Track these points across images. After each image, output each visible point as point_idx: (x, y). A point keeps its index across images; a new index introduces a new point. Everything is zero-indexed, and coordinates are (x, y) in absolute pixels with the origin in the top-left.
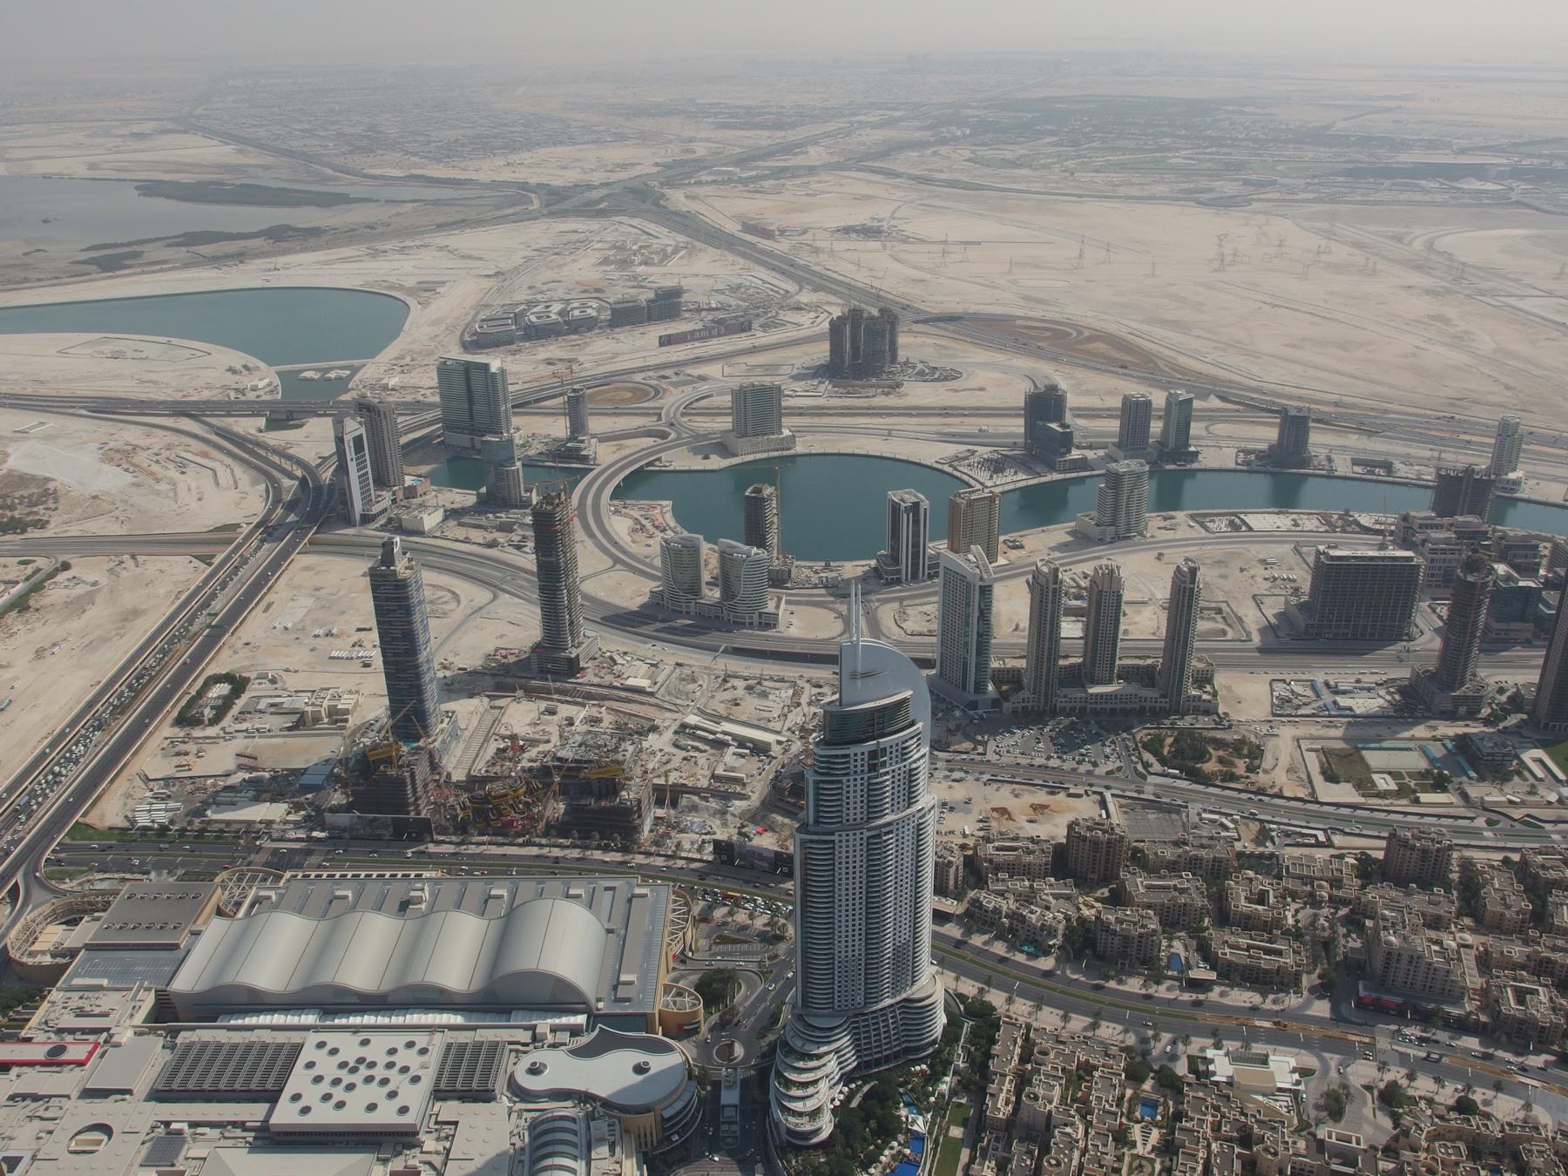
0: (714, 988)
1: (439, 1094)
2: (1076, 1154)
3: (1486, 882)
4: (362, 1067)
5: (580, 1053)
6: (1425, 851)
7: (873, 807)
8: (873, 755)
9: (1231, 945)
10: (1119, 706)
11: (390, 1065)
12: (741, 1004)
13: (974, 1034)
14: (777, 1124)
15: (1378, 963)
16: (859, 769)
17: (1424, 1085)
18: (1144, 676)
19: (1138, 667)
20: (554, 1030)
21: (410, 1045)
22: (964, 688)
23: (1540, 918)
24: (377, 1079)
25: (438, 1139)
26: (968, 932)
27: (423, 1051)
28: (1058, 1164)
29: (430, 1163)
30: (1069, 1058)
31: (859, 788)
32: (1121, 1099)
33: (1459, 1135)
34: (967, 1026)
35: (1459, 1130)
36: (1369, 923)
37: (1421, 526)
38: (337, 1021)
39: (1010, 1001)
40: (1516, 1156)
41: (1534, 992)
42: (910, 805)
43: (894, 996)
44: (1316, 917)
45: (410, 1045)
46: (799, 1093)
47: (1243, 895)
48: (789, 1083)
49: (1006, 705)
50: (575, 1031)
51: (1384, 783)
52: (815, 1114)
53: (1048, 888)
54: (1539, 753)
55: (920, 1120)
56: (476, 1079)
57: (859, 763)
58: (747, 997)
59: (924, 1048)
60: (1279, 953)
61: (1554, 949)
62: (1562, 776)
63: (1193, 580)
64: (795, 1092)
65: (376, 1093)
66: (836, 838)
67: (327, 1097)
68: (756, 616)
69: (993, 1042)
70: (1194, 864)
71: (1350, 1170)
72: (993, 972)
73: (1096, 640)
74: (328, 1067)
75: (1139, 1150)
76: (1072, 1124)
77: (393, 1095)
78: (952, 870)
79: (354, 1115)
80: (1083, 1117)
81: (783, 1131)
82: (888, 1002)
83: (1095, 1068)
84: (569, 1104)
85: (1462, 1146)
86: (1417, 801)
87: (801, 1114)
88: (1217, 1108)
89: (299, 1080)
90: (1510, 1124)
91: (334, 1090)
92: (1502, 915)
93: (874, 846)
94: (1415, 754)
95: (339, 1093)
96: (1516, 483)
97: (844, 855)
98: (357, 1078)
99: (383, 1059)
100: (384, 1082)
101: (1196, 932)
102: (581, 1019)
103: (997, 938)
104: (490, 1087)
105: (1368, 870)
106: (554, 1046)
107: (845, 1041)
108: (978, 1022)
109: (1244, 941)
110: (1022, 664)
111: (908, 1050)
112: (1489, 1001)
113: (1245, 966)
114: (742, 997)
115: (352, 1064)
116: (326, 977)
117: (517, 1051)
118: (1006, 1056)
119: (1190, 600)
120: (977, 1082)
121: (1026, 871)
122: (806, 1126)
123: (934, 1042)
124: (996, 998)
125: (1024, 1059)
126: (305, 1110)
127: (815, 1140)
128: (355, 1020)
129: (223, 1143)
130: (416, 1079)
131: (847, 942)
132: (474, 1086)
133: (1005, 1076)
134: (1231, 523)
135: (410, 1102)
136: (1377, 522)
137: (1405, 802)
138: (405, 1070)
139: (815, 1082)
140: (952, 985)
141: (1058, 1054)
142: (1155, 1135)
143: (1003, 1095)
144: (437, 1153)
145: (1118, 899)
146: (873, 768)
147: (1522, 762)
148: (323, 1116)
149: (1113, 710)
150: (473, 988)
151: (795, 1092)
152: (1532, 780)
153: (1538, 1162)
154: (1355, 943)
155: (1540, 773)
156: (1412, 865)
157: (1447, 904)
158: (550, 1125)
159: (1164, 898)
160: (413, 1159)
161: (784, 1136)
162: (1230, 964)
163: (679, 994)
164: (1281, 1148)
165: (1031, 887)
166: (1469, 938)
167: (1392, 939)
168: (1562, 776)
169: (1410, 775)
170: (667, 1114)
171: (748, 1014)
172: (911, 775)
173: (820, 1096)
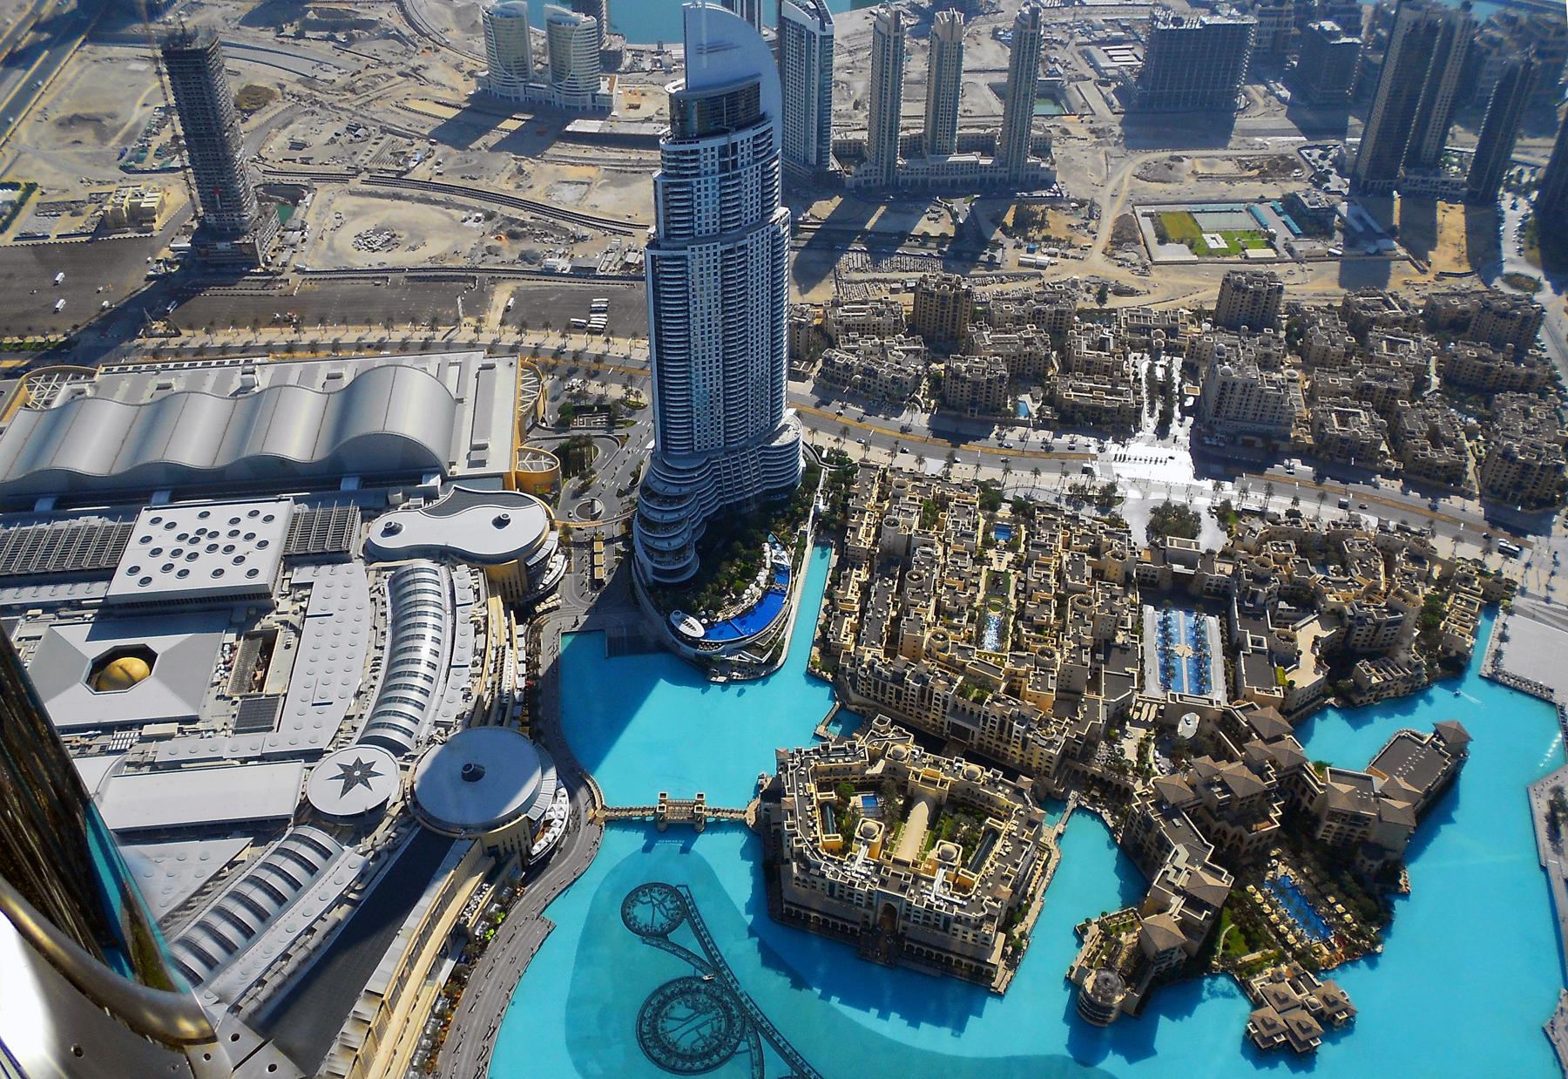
4: (203, 538)
5: (431, 512)
11: (234, 534)
13: (832, 484)
14: (642, 566)
21: (254, 514)
24: (221, 547)
29: (285, 623)
32: (976, 526)
33: (1288, 535)
40: (1340, 550)
45: (254, 514)
52: (679, 552)
60: (1120, 394)
65: (221, 560)
67: (168, 568)
69: (849, 484)
71: (1192, 572)
74: (167, 541)
75: (995, 567)
76: (932, 545)
77: (239, 560)
79: (200, 579)
83: (951, 499)
85: (1292, 544)
88: (1066, 527)
89: (134, 553)
90: (1335, 524)
91: (173, 561)
95: (180, 563)
98: (200, 548)
99: (225, 529)
100: (229, 549)
104: (344, 547)
108: (839, 458)
112: (1317, 426)
116: (154, 455)
124: (854, 452)
125: (879, 500)
126: (146, 581)
129: (57, 621)
130: (263, 544)
132: (327, 547)
133: (863, 512)
135: (264, 567)
142: (1009, 556)
143: (863, 529)
144: (295, 613)
148: (165, 584)
150: (317, 457)
158: (411, 577)
161: (651, 576)
162: (1075, 405)
164: (1128, 552)
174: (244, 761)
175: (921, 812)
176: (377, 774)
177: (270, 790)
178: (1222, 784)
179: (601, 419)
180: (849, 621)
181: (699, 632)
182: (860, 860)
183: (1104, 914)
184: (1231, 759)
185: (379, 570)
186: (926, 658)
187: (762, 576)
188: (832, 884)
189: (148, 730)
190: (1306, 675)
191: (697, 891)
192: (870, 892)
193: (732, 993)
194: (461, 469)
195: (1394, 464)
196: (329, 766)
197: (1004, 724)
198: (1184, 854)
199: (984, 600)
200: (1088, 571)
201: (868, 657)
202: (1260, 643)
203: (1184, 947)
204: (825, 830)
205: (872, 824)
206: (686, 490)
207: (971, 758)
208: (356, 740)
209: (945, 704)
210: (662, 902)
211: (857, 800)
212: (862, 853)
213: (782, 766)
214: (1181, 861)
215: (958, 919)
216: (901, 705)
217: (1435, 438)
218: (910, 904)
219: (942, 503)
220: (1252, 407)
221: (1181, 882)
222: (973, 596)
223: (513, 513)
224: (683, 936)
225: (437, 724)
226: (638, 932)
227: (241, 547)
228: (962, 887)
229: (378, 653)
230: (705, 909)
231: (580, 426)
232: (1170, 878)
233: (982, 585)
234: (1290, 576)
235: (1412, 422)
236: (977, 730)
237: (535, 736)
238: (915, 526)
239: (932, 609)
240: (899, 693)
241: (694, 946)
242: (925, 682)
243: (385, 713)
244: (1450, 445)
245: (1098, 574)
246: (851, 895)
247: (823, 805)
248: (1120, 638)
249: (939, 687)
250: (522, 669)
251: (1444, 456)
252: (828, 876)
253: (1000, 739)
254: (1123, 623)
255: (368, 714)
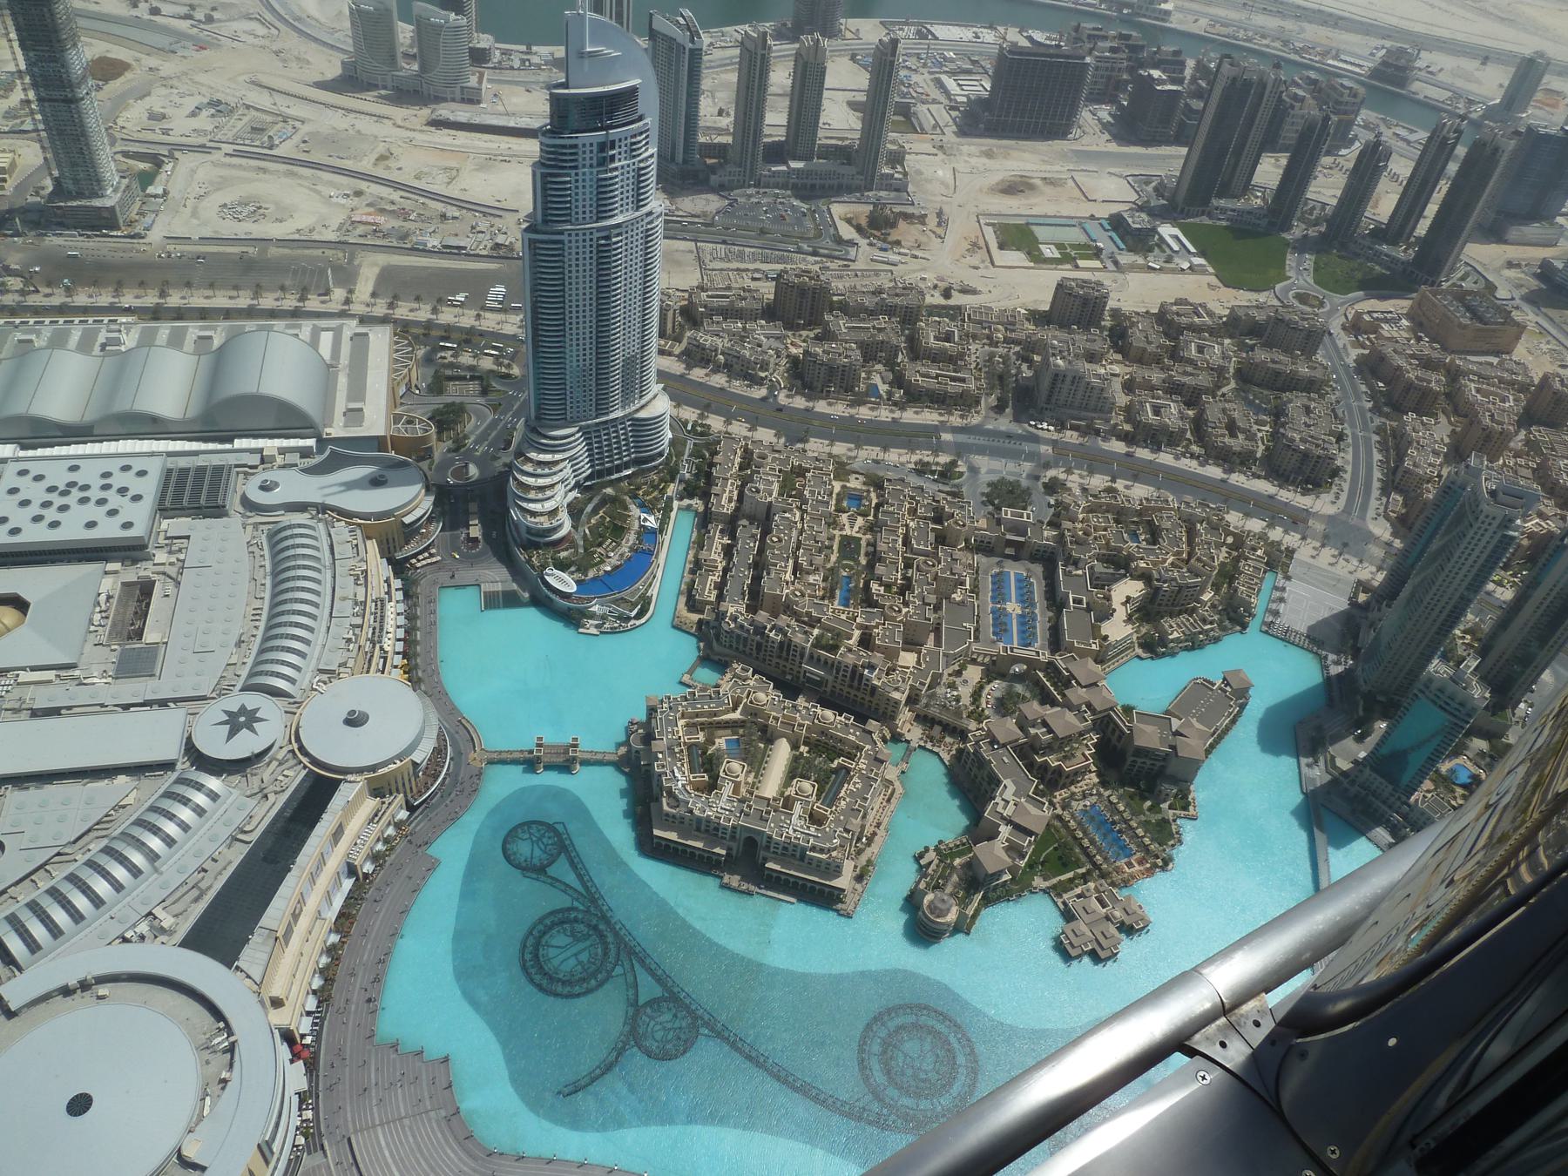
0: (446, 419)
1: (165, 509)
2: (794, 533)
3: (1133, 324)
4: (74, 491)
5: (309, 471)
6: (1085, 301)
7: (602, 211)
8: (602, 147)
9: (920, 374)
10: (818, 182)
11: (106, 487)
12: (472, 432)
13: (696, 453)
14: (516, 525)
15: (1046, 383)
16: (588, 162)
17: (1074, 481)
18: (841, 153)
19: (836, 146)
20: (283, 451)
22: (673, 159)
23: (1174, 354)
24: (93, 500)
25: (170, 552)
26: (689, 367)
27: (142, 473)
28: (780, 540)
30: (782, 462)
31: (588, 190)
34: (690, 445)
35: (1108, 505)
36: (1036, 358)
37: (1089, 36)
38: (40, 452)
39: (728, 422)
40: (1150, 523)
41: (1165, 406)
42: (638, 208)
43: (623, 407)
44: (992, 355)
45: (126, 468)
46: (540, 496)
47: (932, 335)
48: (527, 488)
49: (713, 177)
50: (305, 453)
51: (1049, 251)
52: (553, 513)
53: (761, 330)
54: (1176, 231)
55: (652, 518)
56: (203, 497)
57: (588, 155)
58: (477, 427)
59: (653, 458)
60: (963, 380)
61: (1185, 373)
62: (1192, 249)
63: (894, 53)
64: (532, 495)
66: (565, 238)
67: (37, 519)
68: (458, 91)
69: (717, 453)
70: (890, 311)
72: (709, 401)
73: (799, 114)
75: (848, 532)
77: (113, 513)
78: (670, 314)
79: (72, 530)
80: (800, 508)
81: (523, 530)
82: (619, 414)
84: (307, 515)
86: (1077, 267)
87: (542, 514)
91: (44, 512)
92: (1145, 350)
93: (603, 254)
94: (1076, 230)
95: (51, 514)
96: (1167, 13)
97: (574, 256)
99: (97, 482)
101: (891, 364)
102: (311, 442)
103: (716, 370)
104: (220, 502)
105: (1038, 318)
106: (284, 467)
107: (580, 448)
109: (934, 372)
110: (728, 139)
111: (637, 462)
113: (933, 391)
114: (472, 426)
115: (62, 488)
117: (246, 474)
118: (728, 465)
119: (890, 76)
120: (701, 486)
121: (738, 314)
122: (545, 523)
123: (661, 454)
124: (716, 423)
125: (741, 469)
127: (555, 537)
128: (56, 451)
130: (136, 498)
131: (577, 354)
134: (919, 32)
135: (139, 517)
136: (1048, 38)
137: (1068, 266)
138: (123, 491)
139: (552, 486)
140: (675, 412)
141: (775, 459)
143: (726, 495)
145: (826, 336)
146: (602, 162)
147: (1161, 238)
148: (36, 535)
149: (813, 186)
151: (532, 495)
152: (1168, 252)
153: (1167, 524)
154: (1027, 373)
155: (1176, 247)
156: (1077, 308)
157: (1100, 345)
158: (289, 532)
159: (863, 336)
160: (144, 570)
163: (409, 422)
164: (968, 522)
165: (744, 328)
166: (1117, 369)
167: (1060, 362)
168: (1192, 249)
169: (1073, 246)
170: (407, 520)
171: (476, 442)
172: (639, 174)
173: (558, 498)
174: (126, 707)
175: (781, 754)
176: (262, 720)
177: (157, 736)
178: (1045, 724)
179: (474, 387)
180: (715, 578)
181: (571, 588)
182: (725, 797)
183: (941, 842)
184: (1053, 703)
185: (256, 525)
186: (785, 613)
187: (631, 538)
188: (699, 820)
189: (25, 676)
190: (1117, 629)
191: (571, 828)
192: (734, 827)
193: (604, 918)
194: (336, 430)
195: (1195, 448)
196: (215, 712)
197: (855, 674)
198: (1011, 788)
199: (838, 561)
200: (931, 537)
201: (731, 610)
202: (1079, 602)
203: (1013, 870)
204: (692, 770)
205: (736, 766)
206: (558, 457)
207: (826, 704)
208: (239, 686)
209: (802, 656)
210: (540, 839)
211: (721, 743)
212: (728, 789)
213: (652, 710)
214: (1009, 795)
215: (813, 849)
216: (761, 655)
217: (1232, 428)
218: (770, 837)
219: (801, 472)
220: (1079, 396)
221: (1008, 812)
222: (827, 559)
223: (390, 474)
224: (561, 870)
225: (322, 671)
226: (518, 866)
227: (114, 500)
228: (815, 819)
229: (258, 604)
230: (581, 844)
231: (455, 393)
232: (999, 809)
233: (835, 547)
234: (1108, 543)
235: (1213, 412)
236: (831, 678)
237: (414, 682)
238: (775, 494)
239: (790, 569)
240: (759, 645)
241: (571, 879)
242: (785, 634)
243: (266, 662)
244: (1244, 431)
245: (941, 539)
246: (716, 829)
247: (690, 747)
248: (957, 597)
249: (798, 638)
250: (402, 620)
251: (1238, 443)
252: (696, 812)
253: (851, 686)
254: (963, 583)
255: (250, 661)
